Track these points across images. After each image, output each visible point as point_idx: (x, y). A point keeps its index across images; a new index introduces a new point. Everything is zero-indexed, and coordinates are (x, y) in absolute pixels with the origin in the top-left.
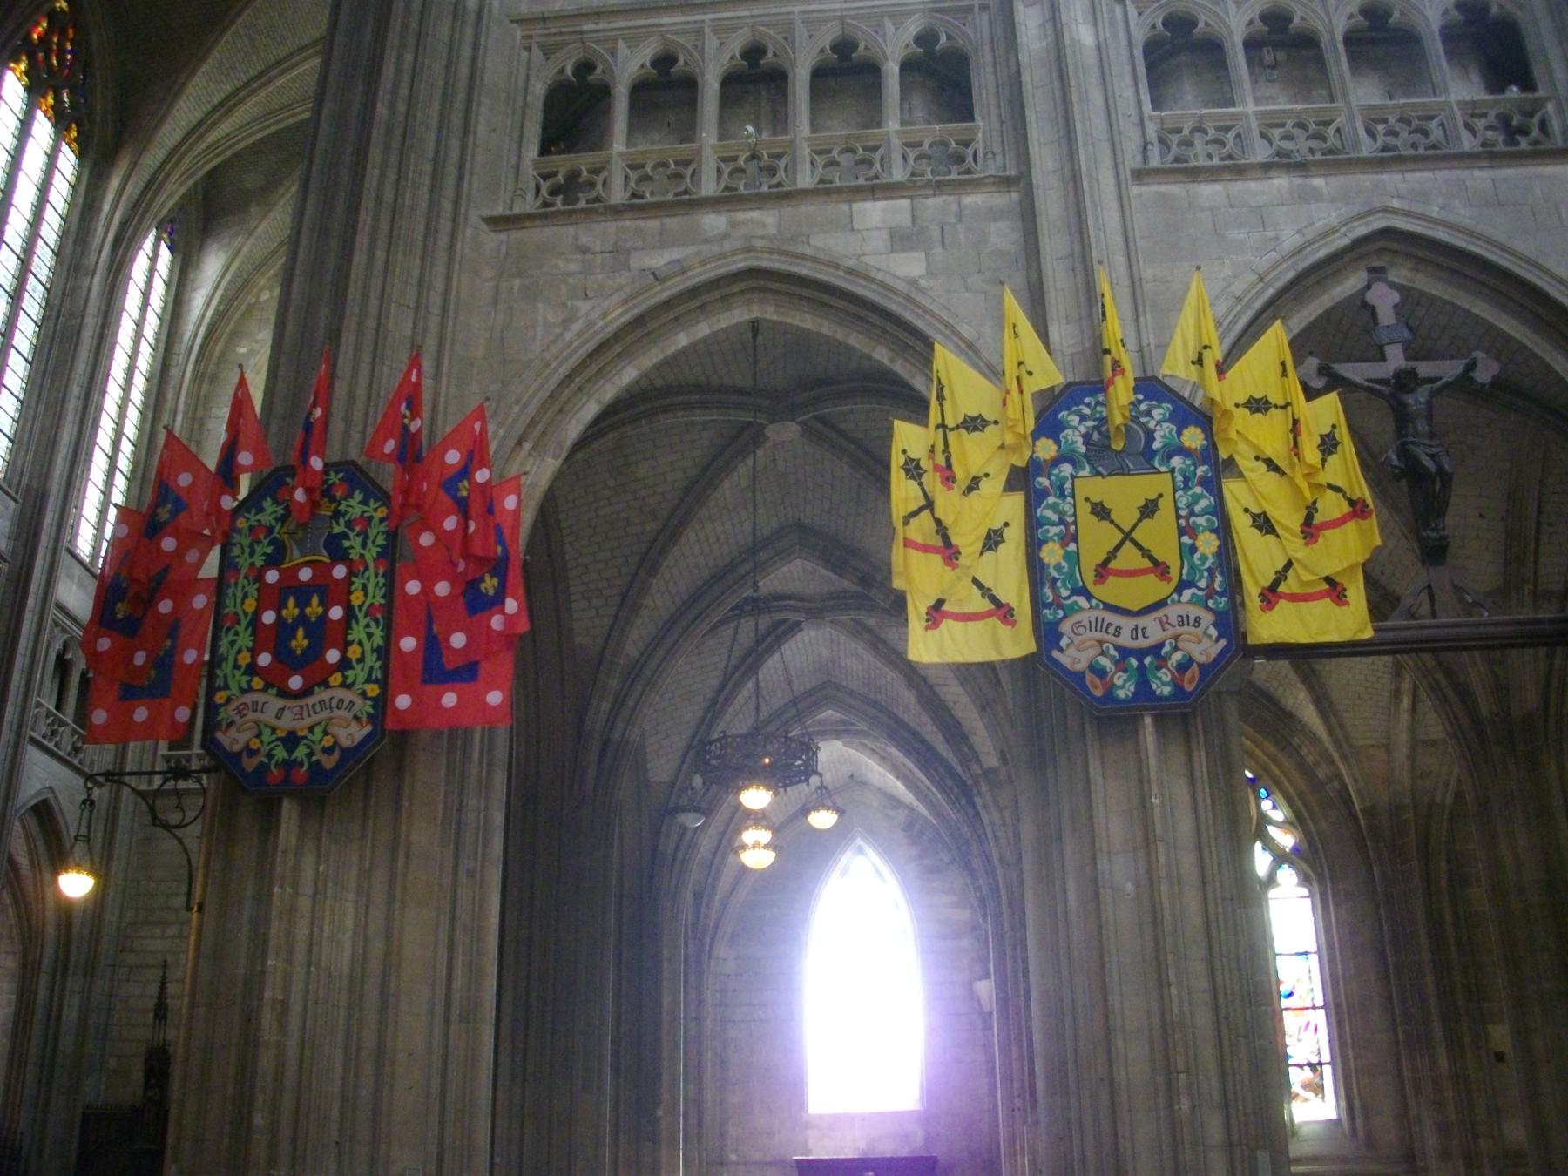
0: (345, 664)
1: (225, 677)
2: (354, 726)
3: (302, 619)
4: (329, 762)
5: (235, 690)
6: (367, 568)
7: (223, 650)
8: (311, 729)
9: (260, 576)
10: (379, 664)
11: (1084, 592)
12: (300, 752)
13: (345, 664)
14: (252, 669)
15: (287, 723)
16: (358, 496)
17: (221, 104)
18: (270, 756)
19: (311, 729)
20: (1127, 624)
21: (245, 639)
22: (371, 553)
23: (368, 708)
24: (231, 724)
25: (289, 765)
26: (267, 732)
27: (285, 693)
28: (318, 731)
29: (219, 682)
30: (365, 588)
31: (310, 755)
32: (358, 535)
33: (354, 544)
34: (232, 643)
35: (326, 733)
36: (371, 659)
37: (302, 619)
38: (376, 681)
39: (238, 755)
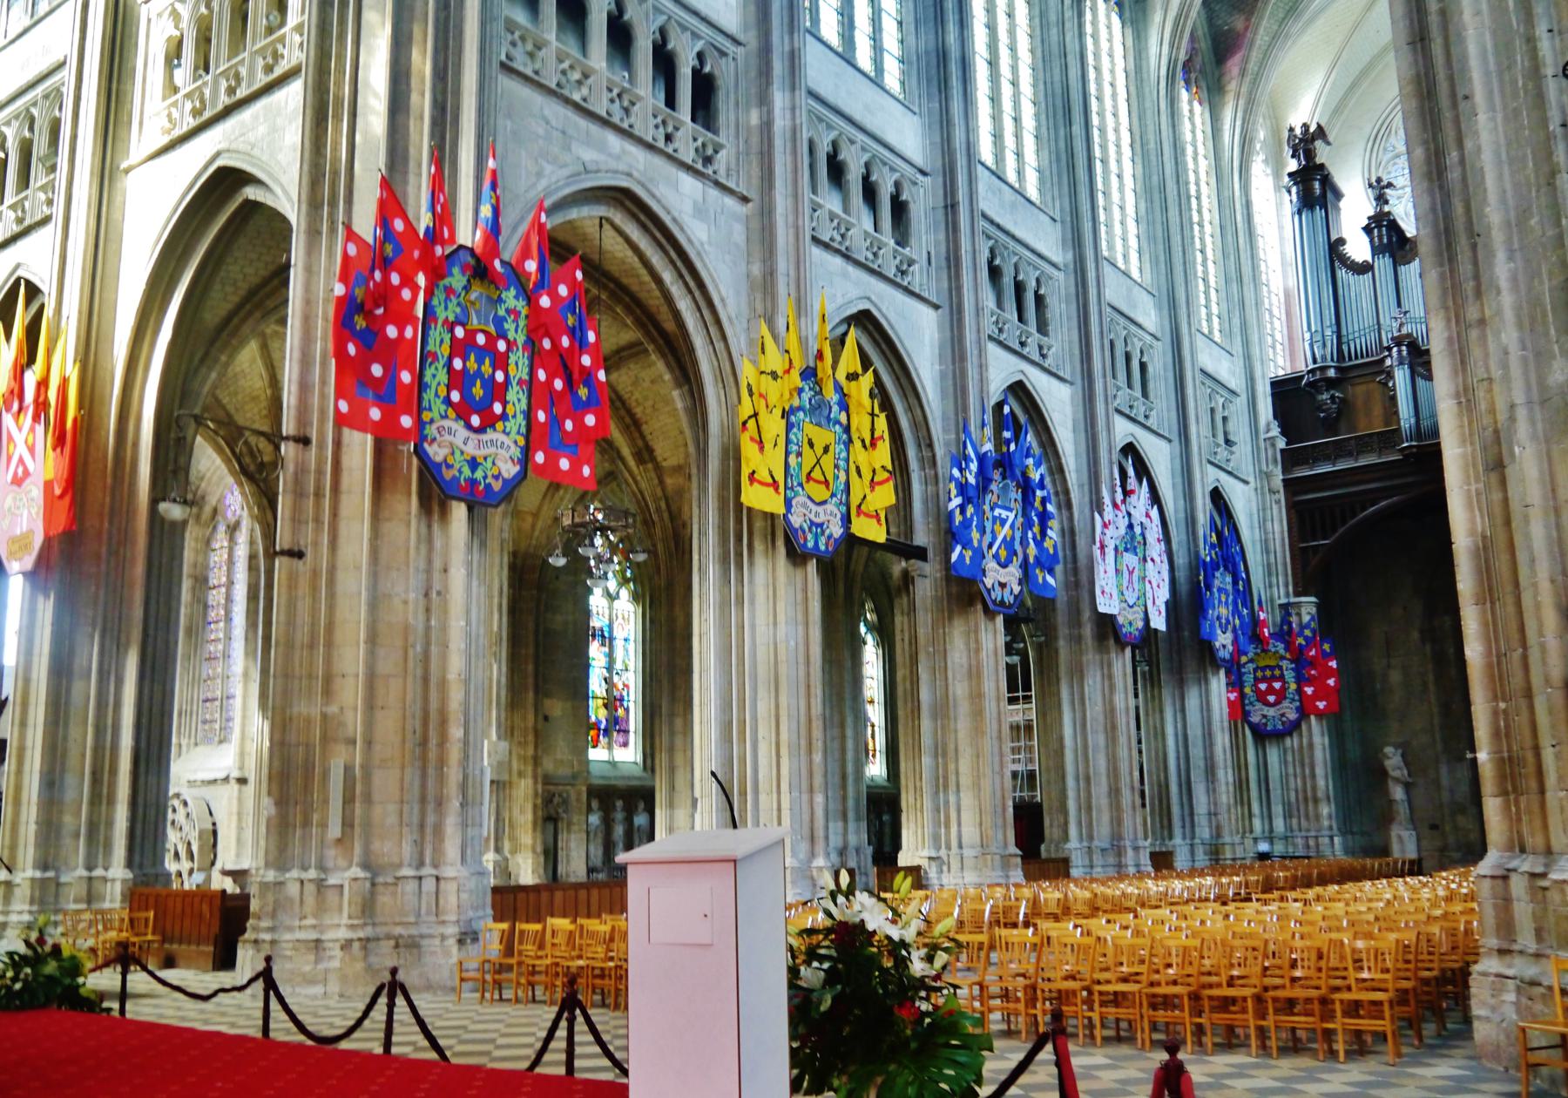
5: (435, 414)
7: (428, 378)
11: (801, 485)
12: (479, 474)
13: (504, 417)
14: (447, 401)
15: (471, 450)
18: (460, 472)
20: (814, 508)
21: (443, 377)
24: (434, 440)
27: (469, 426)
28: (490, 460)
29: (425, 404)
31: (485, 478)
33: (509, 326)
36: (520, 418)
37: (478, 373)
39: (439, 465)
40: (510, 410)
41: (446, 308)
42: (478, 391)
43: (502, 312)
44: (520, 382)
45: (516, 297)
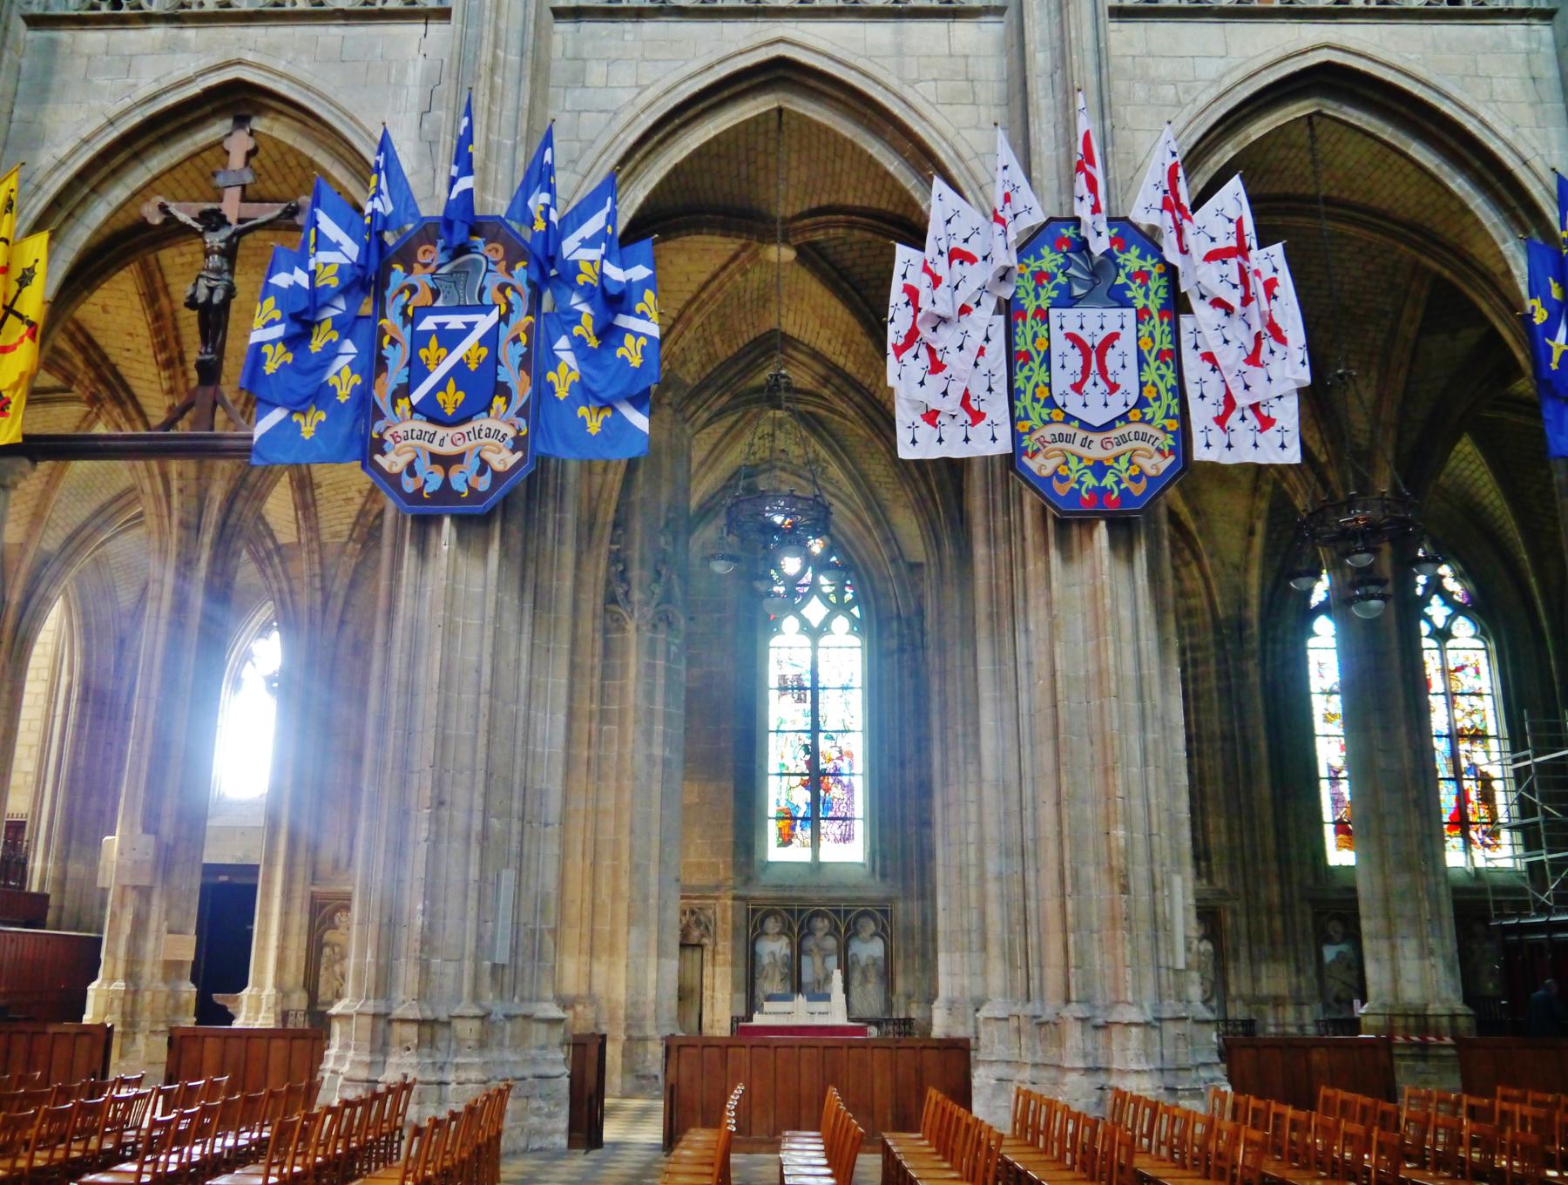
1: (1025, 408)
2: (1157, 458)
4: (1138, 489)
5: (1036, 422)
6: (1151, 318)
7: (1020, 382)
8: (1117, 459)
10: (1176, 401)
12: (1109, 481)
15: (1096, 452)
16: (1135, 251)
18: (1081, 483)
19: (1117, 459)
25: (1100, 493)
26: (1073, 462)
30: (1151, 335)
31: (1118, 483)
32: (1140, 287)
33: (1135, 292)
34: (1028, 378)
35: (1131, 462)
36: (1167, 398)
38: (1174, 417)
39: (1050, 478)
41: (1037, 297)
43: (1121, 280)
44: (1161, 355)
45: (1142, 257)
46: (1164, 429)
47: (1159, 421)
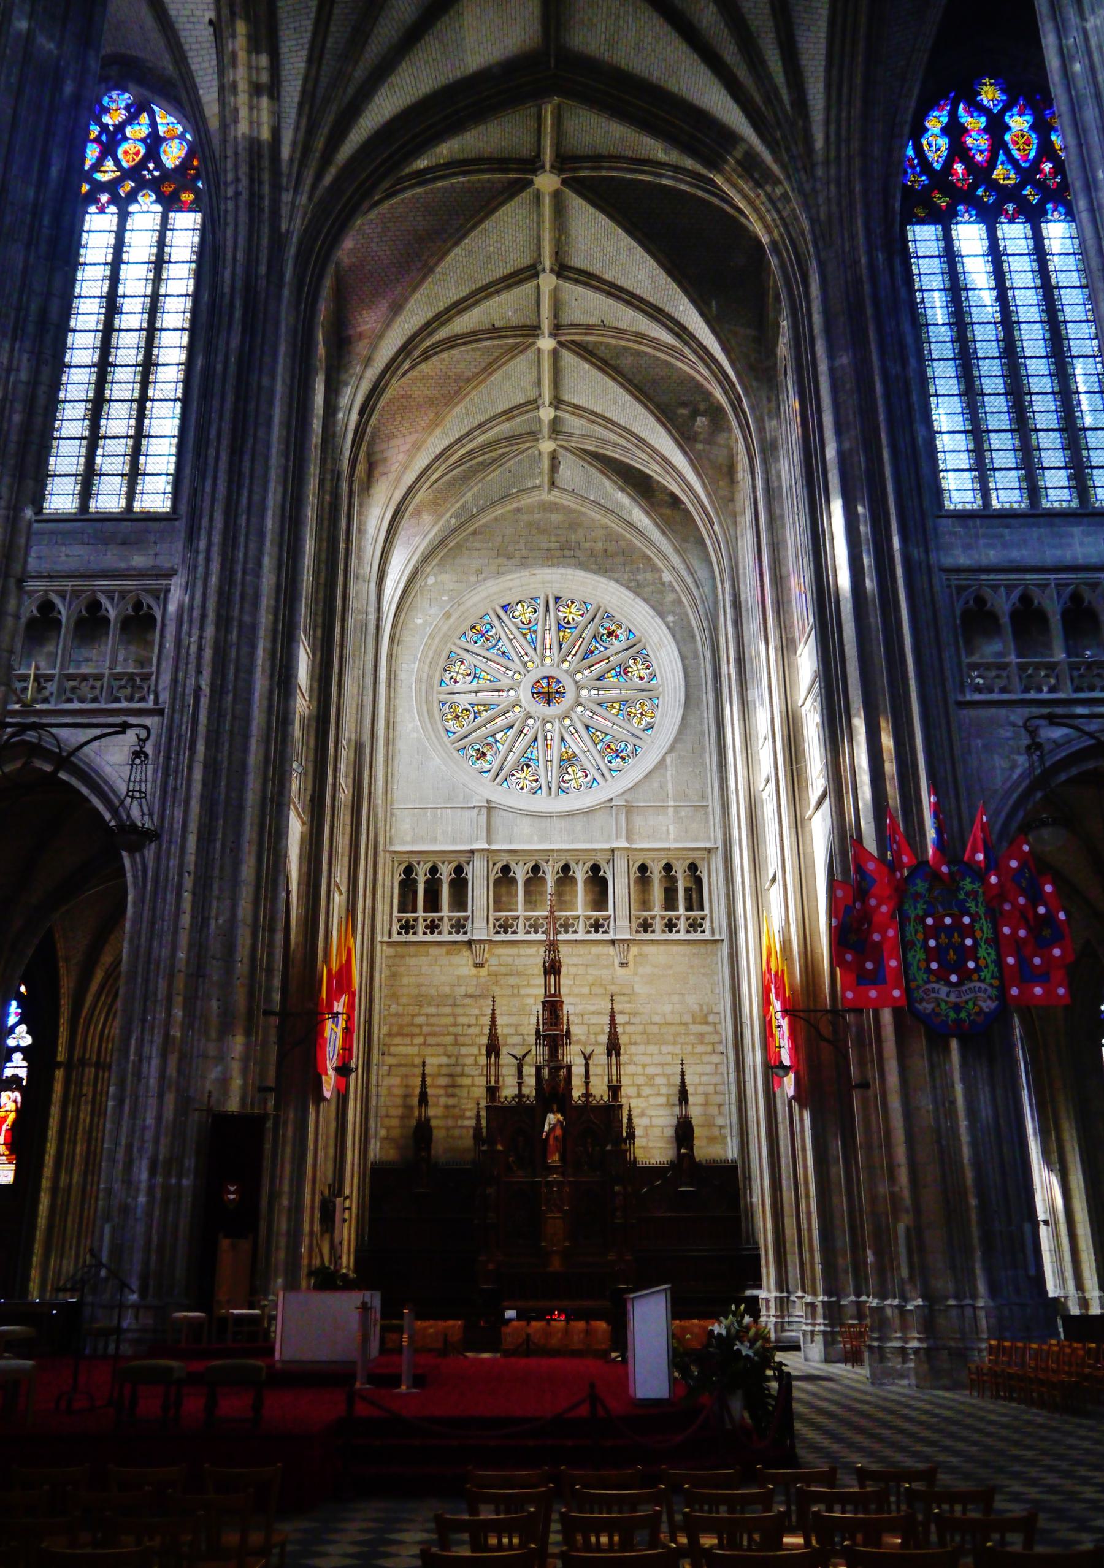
0: (978, 969)
2: (989, 1002)
3: (950, 945)
8: (967, 1002)
9: (921, 920)
12: (963, 1015)
14: (928, 970)
15: (953, 998)
16: (968, 880)
17: (441, 454)
18: (947, 1016)
19: (967, 1002)
21: (921, 955)
22: (982, 910)
23: (994, 992)
28: (971, 1005)
30: (982, 929)
31: (969, 1016)
35: (975, 1004)
36: (992, 967)
40: (982, 963)
42: (952, 955)
43: (962, 896)
44: (987, 941)
45: (972, 882)
46: (991, 985)
47: (988, 980)
